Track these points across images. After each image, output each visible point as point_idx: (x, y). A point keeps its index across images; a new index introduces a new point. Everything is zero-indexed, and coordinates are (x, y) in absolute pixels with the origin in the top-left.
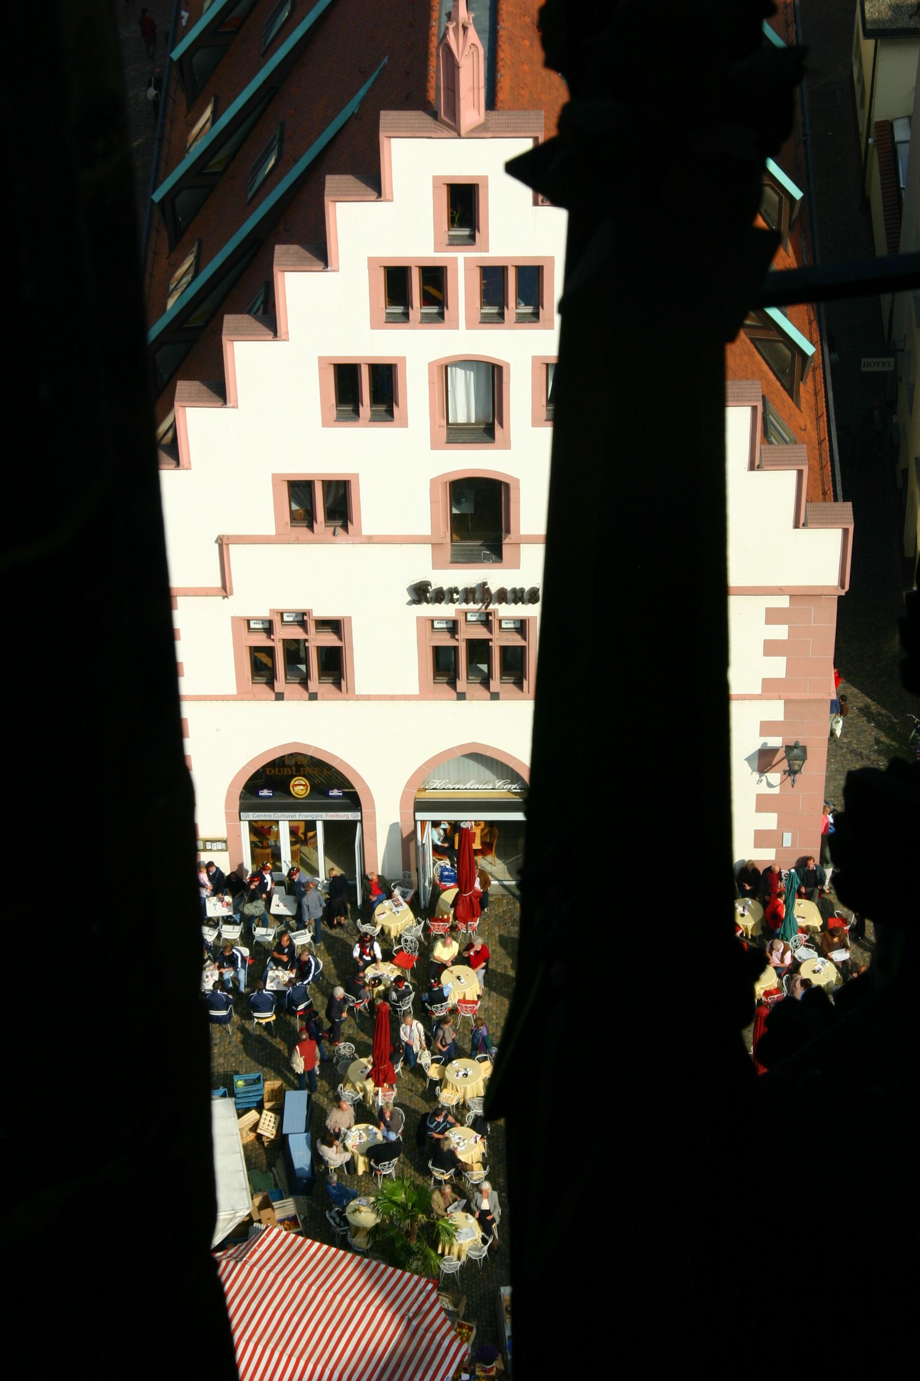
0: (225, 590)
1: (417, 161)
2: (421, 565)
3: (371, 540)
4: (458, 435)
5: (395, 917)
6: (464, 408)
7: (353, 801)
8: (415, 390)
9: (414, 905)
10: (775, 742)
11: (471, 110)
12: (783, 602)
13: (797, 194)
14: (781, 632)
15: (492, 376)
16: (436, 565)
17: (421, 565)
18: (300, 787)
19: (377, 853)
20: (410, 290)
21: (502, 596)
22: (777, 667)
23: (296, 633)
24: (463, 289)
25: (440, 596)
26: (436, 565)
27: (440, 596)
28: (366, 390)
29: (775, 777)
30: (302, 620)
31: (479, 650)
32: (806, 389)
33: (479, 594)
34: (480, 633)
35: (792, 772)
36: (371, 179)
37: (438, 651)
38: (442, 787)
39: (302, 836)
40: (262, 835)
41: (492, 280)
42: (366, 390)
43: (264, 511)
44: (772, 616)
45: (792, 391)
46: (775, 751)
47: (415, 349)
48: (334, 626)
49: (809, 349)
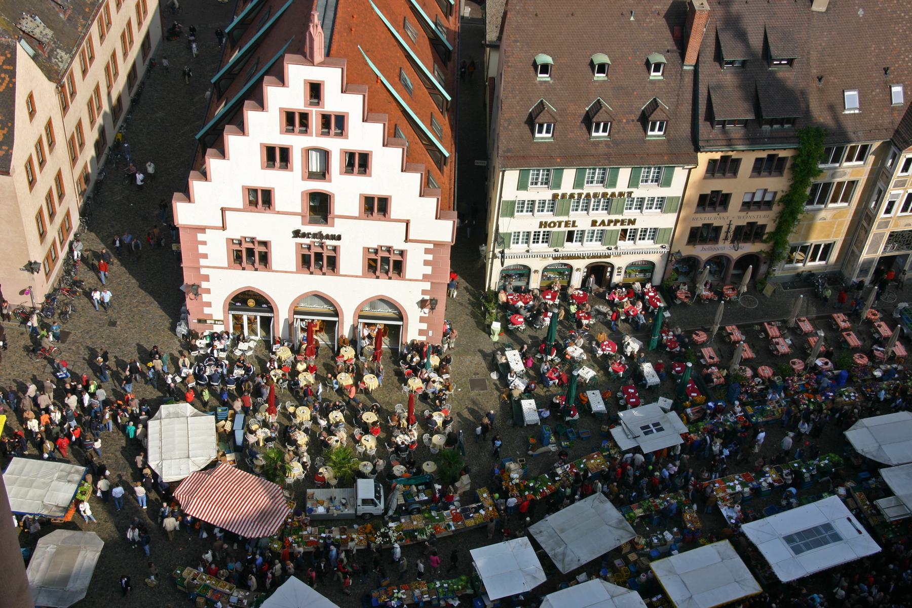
0: (224, 228)
1: (298, 74)
2: (297, 223)
3: (278, 213)
4: (312, 176)
5: (284, 353)
6: (315, 166)
7: (271, 309)
8: (296, 158)
9: (292, 349)
10: (427, 297)
11: (319, 56)
12: (431, 246)
13: (449, 98)
14: (430, 257)
15: (325, 155)
16: (303, 224)
17: (297, 223)
18: (251, 303)
19: (279, 329)
20: (294, 121)
21: (327, 237)
22: (428, 270)
23: (250, 246)
24: (315, 122)
25: (304, 235)
26: (303, 224)
27: (304, 235)
28: (277, 157)
29: (427, 310)
30: (253, 240)
31: (319, 256)
32: (446, 169)
33: (319, 235)
34: (319, 250)
35: (432, 309)
36: (281, 80)
37: (304, 256)
38: (303, 306)
39: (251, 322)
40: (237, 319)
41: (326, 120)
42: (277, 157)
43: (238, 200)
44: (427, 251)
45: (441, 169)
46: (426, 301)
47: (297, 143)
48: (265, 244)
49: (447, 155)
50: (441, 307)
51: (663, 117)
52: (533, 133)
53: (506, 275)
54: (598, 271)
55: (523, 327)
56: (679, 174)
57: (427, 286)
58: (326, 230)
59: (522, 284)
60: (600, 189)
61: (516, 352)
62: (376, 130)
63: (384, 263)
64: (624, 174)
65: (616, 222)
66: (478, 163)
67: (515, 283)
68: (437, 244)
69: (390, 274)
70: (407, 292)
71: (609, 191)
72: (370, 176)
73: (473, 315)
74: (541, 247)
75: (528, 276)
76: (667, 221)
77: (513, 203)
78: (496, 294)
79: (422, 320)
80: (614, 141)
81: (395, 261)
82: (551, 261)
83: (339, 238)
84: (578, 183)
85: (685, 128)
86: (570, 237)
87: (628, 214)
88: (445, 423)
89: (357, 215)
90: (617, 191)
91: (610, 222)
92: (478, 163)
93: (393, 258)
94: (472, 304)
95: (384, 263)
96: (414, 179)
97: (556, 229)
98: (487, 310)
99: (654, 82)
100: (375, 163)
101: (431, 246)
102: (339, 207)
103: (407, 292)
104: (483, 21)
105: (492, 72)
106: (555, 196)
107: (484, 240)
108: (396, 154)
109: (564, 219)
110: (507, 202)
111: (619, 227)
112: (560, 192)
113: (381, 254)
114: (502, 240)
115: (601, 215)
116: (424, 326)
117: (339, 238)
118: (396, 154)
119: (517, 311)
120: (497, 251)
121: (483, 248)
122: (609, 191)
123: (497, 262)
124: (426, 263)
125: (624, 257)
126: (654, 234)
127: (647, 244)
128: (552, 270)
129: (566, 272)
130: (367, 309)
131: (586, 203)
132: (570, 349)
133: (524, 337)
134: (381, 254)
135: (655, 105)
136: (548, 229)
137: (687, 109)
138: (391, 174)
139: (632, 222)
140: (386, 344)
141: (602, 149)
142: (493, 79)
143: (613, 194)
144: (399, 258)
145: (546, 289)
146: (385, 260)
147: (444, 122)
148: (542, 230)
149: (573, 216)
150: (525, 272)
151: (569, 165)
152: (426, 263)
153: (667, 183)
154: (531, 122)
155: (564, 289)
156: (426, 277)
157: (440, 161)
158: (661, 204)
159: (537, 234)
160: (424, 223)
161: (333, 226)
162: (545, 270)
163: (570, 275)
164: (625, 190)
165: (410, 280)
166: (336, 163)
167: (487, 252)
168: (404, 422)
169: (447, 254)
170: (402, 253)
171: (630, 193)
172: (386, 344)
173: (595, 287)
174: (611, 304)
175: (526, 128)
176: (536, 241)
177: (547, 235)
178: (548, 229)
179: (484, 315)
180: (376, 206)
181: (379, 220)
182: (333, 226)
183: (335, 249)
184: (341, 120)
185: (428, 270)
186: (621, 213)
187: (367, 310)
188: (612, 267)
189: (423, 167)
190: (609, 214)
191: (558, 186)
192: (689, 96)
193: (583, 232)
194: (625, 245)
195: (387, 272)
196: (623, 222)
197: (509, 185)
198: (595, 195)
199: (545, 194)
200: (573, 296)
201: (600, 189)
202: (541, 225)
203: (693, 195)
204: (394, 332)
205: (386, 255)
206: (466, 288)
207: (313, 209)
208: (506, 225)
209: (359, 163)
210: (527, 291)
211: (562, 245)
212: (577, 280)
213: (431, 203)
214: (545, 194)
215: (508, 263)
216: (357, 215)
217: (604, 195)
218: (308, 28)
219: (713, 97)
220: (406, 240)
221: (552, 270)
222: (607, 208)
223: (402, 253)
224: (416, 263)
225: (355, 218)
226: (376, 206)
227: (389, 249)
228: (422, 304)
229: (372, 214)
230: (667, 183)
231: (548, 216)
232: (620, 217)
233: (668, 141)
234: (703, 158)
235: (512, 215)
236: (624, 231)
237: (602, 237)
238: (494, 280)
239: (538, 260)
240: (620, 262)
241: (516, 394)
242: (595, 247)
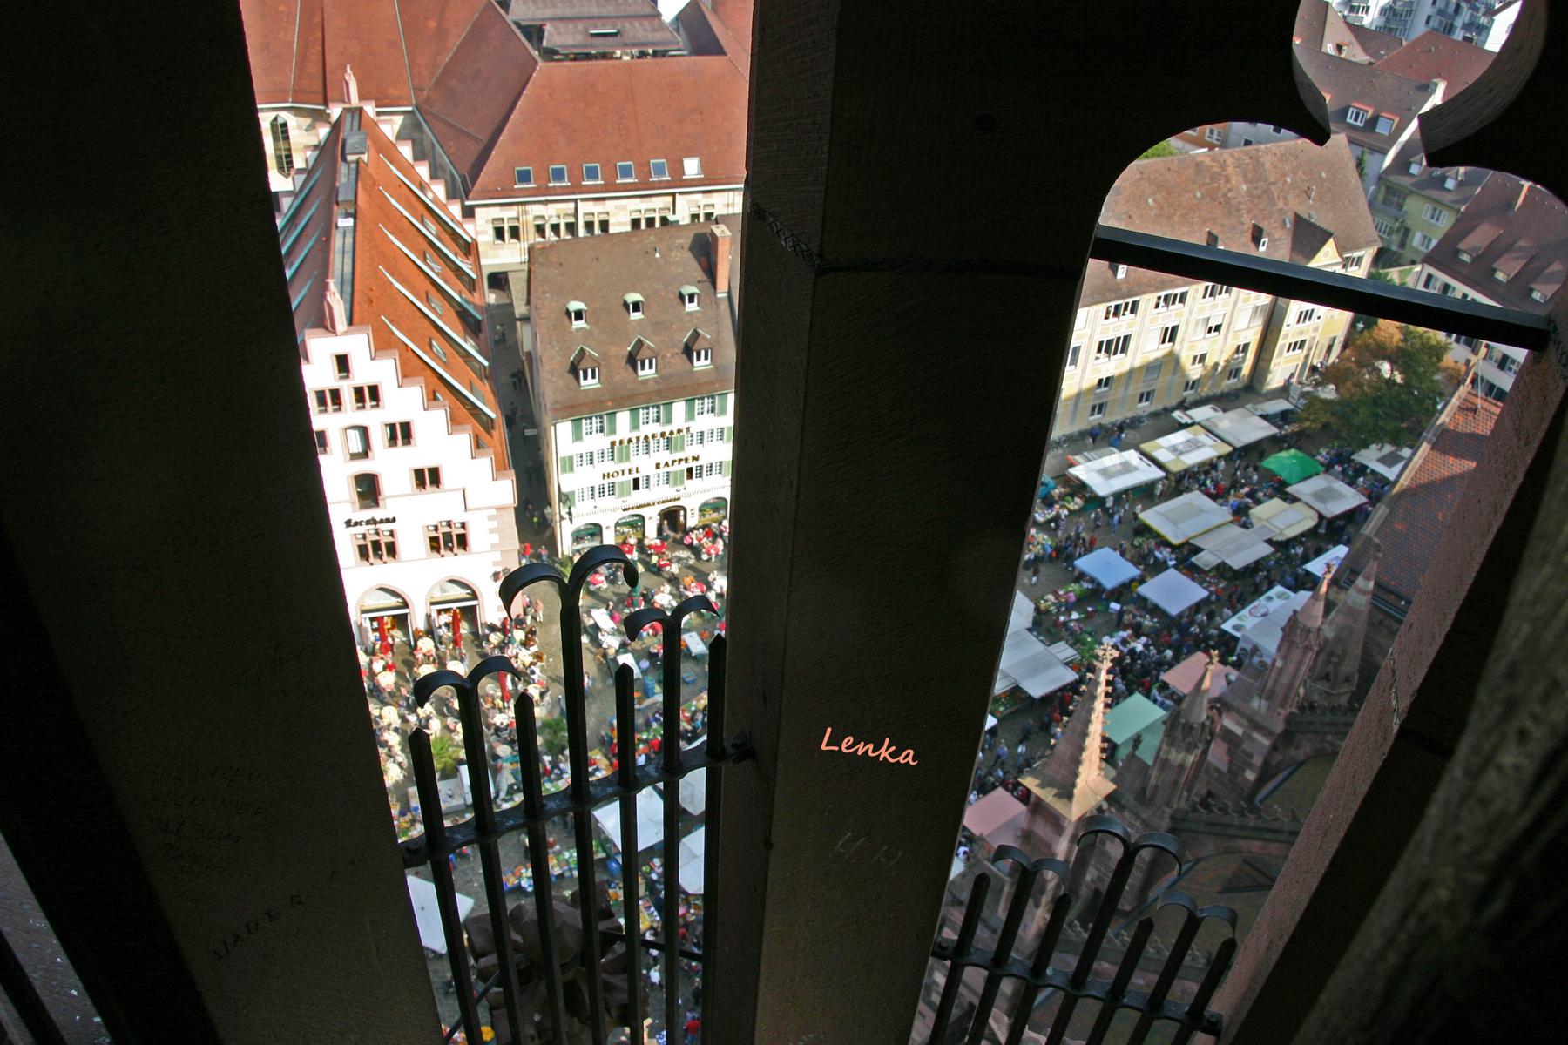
13: (486, 363)
14: (494, 524)
21: (381, 521)
22: (495, 538)
25: (356, 524)
27: (356, 524)
31: (376, 544)
32: (495, 433)
33: (372, 521)
34: (376, 538)
44: (490, 518)
45: (489, 433)
49: (493, 416)
51: (707, 345)
55: (605, 585)
58: (376, 513)
60: (657, 429)
61: (603, 610)
63: (448, 540)
64: (679, 408)
68: (498, 509)
74: (609, 501)
77: (571, 458)
80: (662, 377)
84: (635, 426)
87: (689, 451)
88: (542, 695)
95: (448, 540)
99: (690, 314)
101: (493, 512)
102: (386, 487)
104: (511, 304)
106: (613, 443)
109: (625, 466)
112: (616, 438)
114: (566, 498)
115: (664, 456)
121: (548, 511)
122: (667, 429)
123: (566, 523)
124: (492, 531)
128: (625, 524)
132: (657, 598)
133: (608, 595)
135: (696, 335)
136: (611, 480)
140: (464, 628)
141: (652, 386)
144: (462, 531)
146: (448, 537)
147: (486, 387)
148: (607, 481)
149: (635, 461)
150: (595, 530)
152: (492, 531)
154: (574, 370)
157: (488, 424)
160: (482, 491)
166: (379, 437)
168: (499, 702)
169: (511, 518)
172: (464, 628)
173: (672, 534)
174: (690, 547)
175: (571, 377)
176: (602, 494)
178: (611, 480)
180: (428, 478)
183: (392, 534)
184: (374, 391)
185: (495, 538)
189: (469, 427)
191: (613, 431)
197: (562, 439)
198: (654, 436)
201: (657, 429)
204: (470, 613)
207: (361, 495)
217: (663, 434)
218: (324, 296)
221: (625, 524)
223: (463, 525)
226: (428, 478)
231: (610, 466)
233: (716, 368)
236: (690, 470)
239: (608, 514)
241: (611, 652)
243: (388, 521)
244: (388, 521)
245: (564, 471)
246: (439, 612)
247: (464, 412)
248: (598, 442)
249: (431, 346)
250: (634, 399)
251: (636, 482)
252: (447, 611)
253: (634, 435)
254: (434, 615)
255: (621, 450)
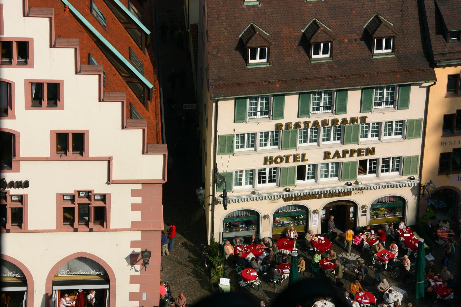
10: (138, 250)
12: (139, 187)
13: (148, 32)
14: (138, 200)
22: (137, 216)
32: (151, 104)
35: (145, 264)
44: (135, 193)
45: (144, 104)
46: (137, 255)
49: (150, 86)
50: (156, 261)
51: (389, 33)
52: (246, 60)
53: (230, 224)
54: (340, 213)
55: (257, 283)
56: (417, 94)
57: (137, 236)
59: (250, 233)
60: (329, 116)
62: (67, 56)
64: (354, 98)
65: (352, 152)
66: (187, 107)
67: (242, 233)
68: (145, 183)
69: (91, 225)
70: (112, 246)
71: (340, 117)
72: (62, 108)
73: (196, 274)
74: (268, 187)
75: (257, 223)
76: (409, 148)
77: (231, 137)
78: (221, 248)
79: (133, 280)
81: (96, 208)
82: (281, 204)
83: (26, 185)
84: (303, 110)
85: (416, 44)
86: (301, 176)
89: (48, 155)
90: (348, 116)
91: (345, 152)
92: (187, 107)
93: (95, 204)
94: (192, 261)
95: (83, 212)
96: (115, 109)
97: (283, 165)
98: (212, 266)
100: (67, 94)
102: (24, 148)
103: (112, 246)
105: (194, 18)
106: (278, 127)
107: (201, 182)
108: (91, 82)
109: (291, 152)
110: (223, 137)
111: (356, 158)
112: (283, 122)
113: (78, 201)
114: (222, 181)
115: (334, 145)
116: (136, 288)
117: (26, 185)
118: (91, 82)
119: (248, 265)
120: (218, 195)
122: (340, 117)
123: (219, 208)
124: (135, 207)
125: (367, 193)
126: (399, 163)
127: (392, 176)
128: (285, 215)
129: (301, 215)
130: (64, 272)
131: (315, 132)
134: (78, 201)
135: (377, 22)
136: (274, 165)
137: (413, 24)
138: (86, 104)
139: (371, 151)
142: (195, 27)
143: (344, 121)
144: (101, 204)
145: (280, 238)
147: (145, 57)
148: (268, 166)
149: (302, 148)
150: (252, 219)
151: (290, 90)
152: (135, 207)
153: (405, 104)
155: (301, 236)
156: (135, 226)
157: (143, 94)
158: (402, 128)
159: (262, 173)
160: (128, 161)
161: (18, 170)
162: (277, 214)
163: (307, 219)
164: (358, 115)
165: (116, 230)
167: (206, 197)
169: (158, 195)
170: (104, 198)
171: (363, 119)
175: (238, 55)
176: (262, 180)
177: (274, 171)
178: (274, 165)
179: (208, 272)
180: (71, 144)
181: (75, 160)
182: (18, 170)
183: (21, 199)
185: (137, 216)
186: (356, 140)
187: (63, 274)
188: (355, 205)
190: (342, 143)
191: (280, 115)
192: (414, 11)
193: (315, 166)
194: (366, 179)
195: (87, 224)
196: (360, 152)
197: (224, 117)
198: (324, 123)
199: (268, 125)
200: (313, 243)
201: (329, 116)
202: (266, 161)
203: (436, 114)
205: (86, 201)
206: (185, 245)
208: (225, 163)
209: (47, 94)
210: (258, 241)
211: (293, 183)
212: (315, 224)
213: (136, 136)
214: (268, 125)
215: (233, 208)
216: (47, 154)
217: (335, 122)
219: (442, 9)
220: (109, 181)
221: (285, 215)
222: (339, 137)
223: (104, 198)
224: (123, 209)
225: (46, 159)
226: (71, 144)
227: (88, 194)
228: (133, 259)
229: (66, 154)
230: (405, 104)
232: (355, 147)
233: (398, 58)
234: (442, 74)
235: (231, 151)
236: (363, 163)
237: (338, 171)
238: (217, 230)
240: (364, 200)
242: (331, 183)
243: (19, 185)
244: (19, 185)
245: (222, 152)
246: (63, 294)
247: (119, 79)
248: (264, 125)
249: (91, 8)
250: (308, 84)
251: (301, 170)
252: (70, 293)
253: (303, 120)
254: (56, 296)
255: (287, 134)
